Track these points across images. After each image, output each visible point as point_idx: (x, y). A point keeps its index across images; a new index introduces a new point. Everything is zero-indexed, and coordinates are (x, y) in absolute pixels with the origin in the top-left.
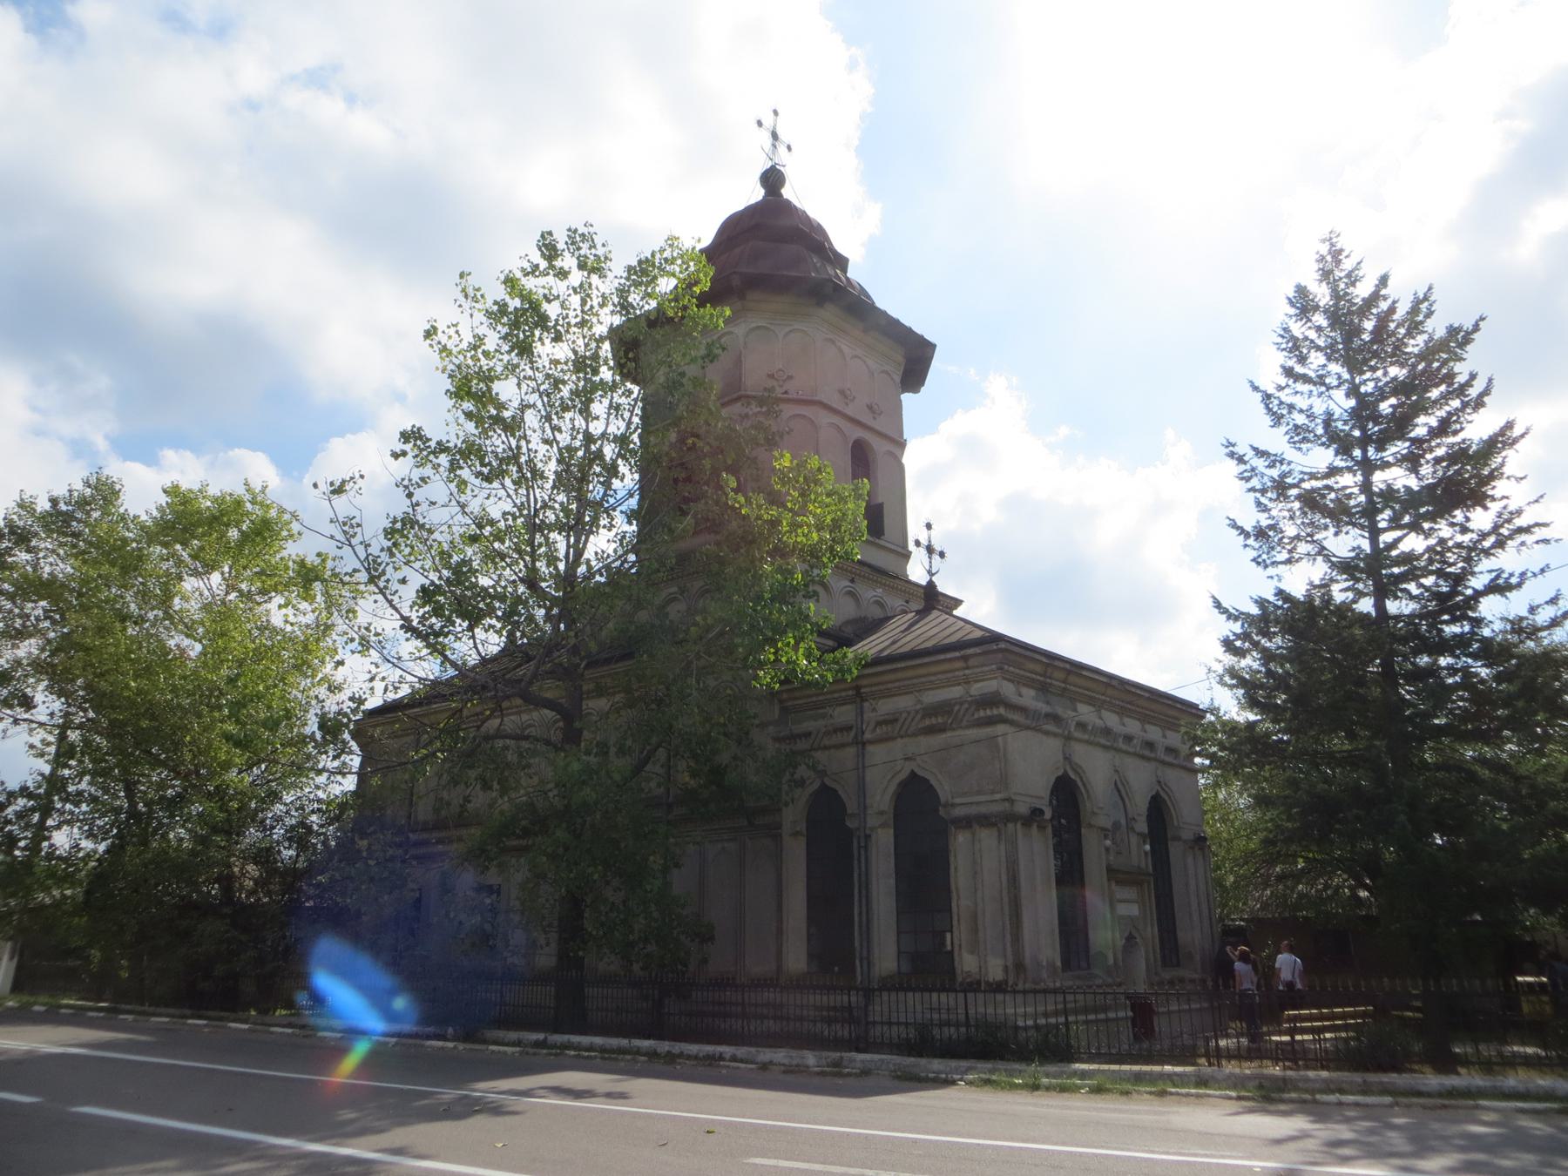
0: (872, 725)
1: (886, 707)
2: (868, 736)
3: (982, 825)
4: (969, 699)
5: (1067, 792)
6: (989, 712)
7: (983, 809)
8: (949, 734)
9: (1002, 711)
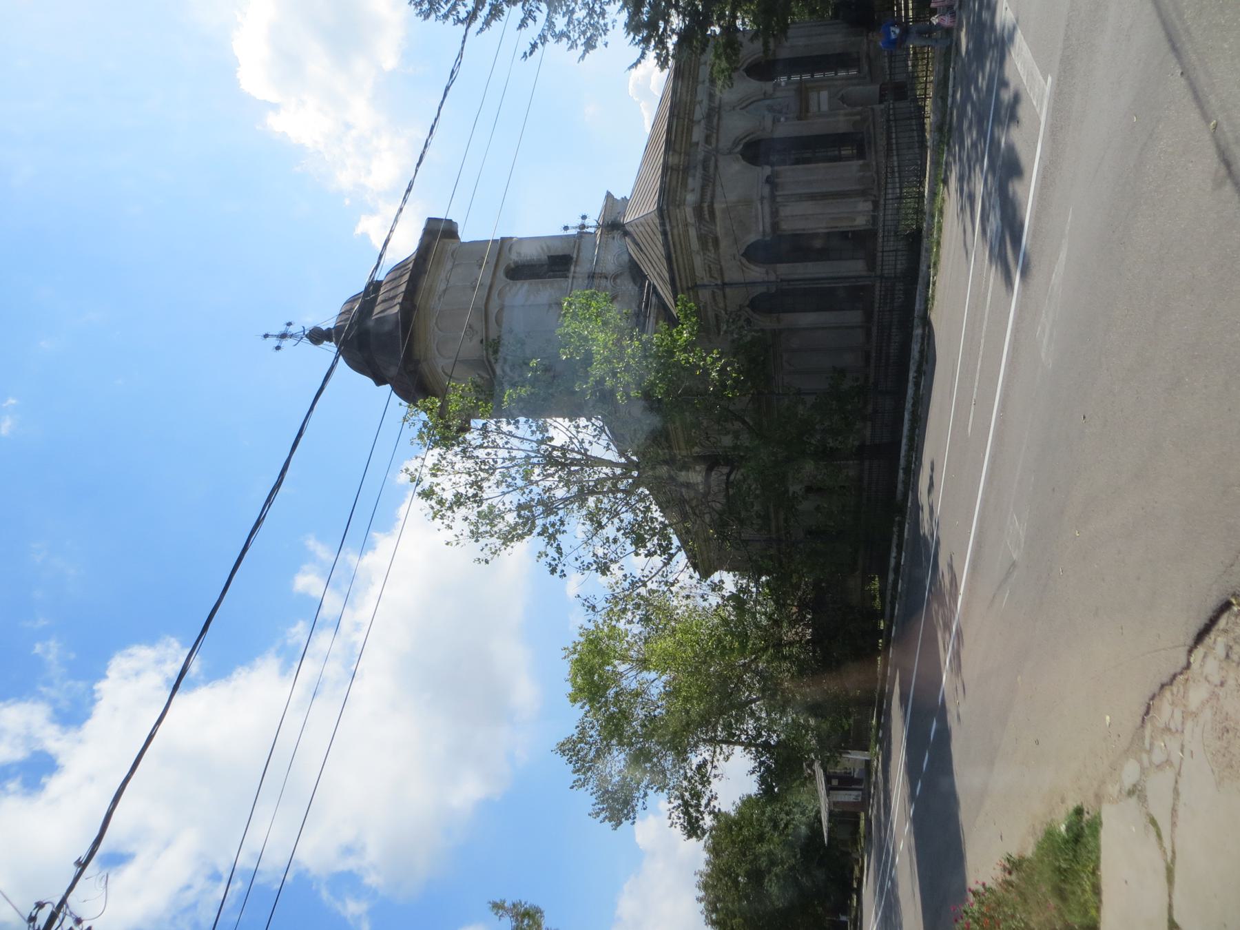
0: (713, 280)
1: (700, 272)
2: (719, 282)
4: (697, 224)
5: (754, 151)
6: (706, 213)
9: (705, 205)
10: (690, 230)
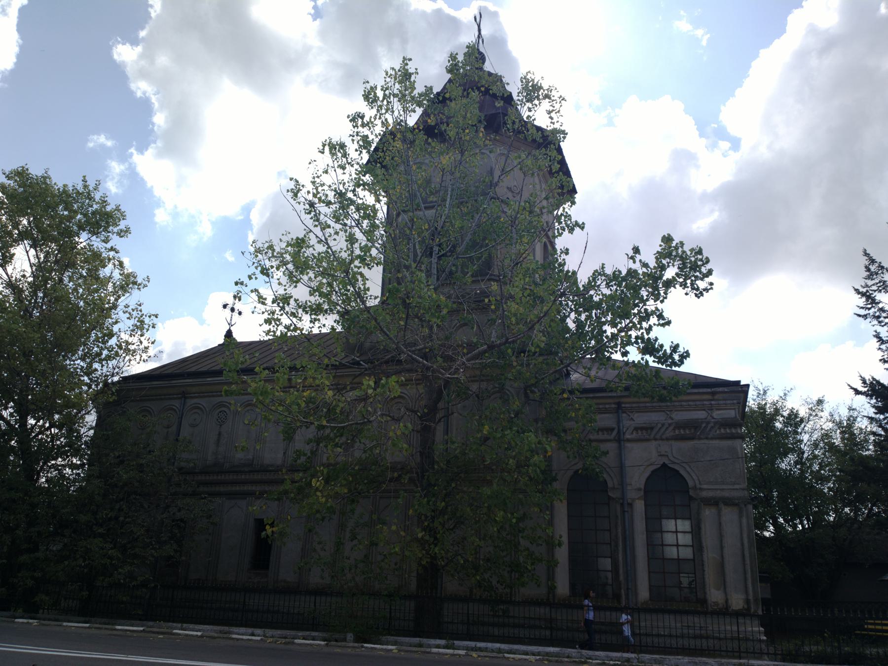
1: (641, 419)
2: (628, 436)
3: (726, 504)
7: (726, 494)
8: (696, 442)
10: (704, 412)
